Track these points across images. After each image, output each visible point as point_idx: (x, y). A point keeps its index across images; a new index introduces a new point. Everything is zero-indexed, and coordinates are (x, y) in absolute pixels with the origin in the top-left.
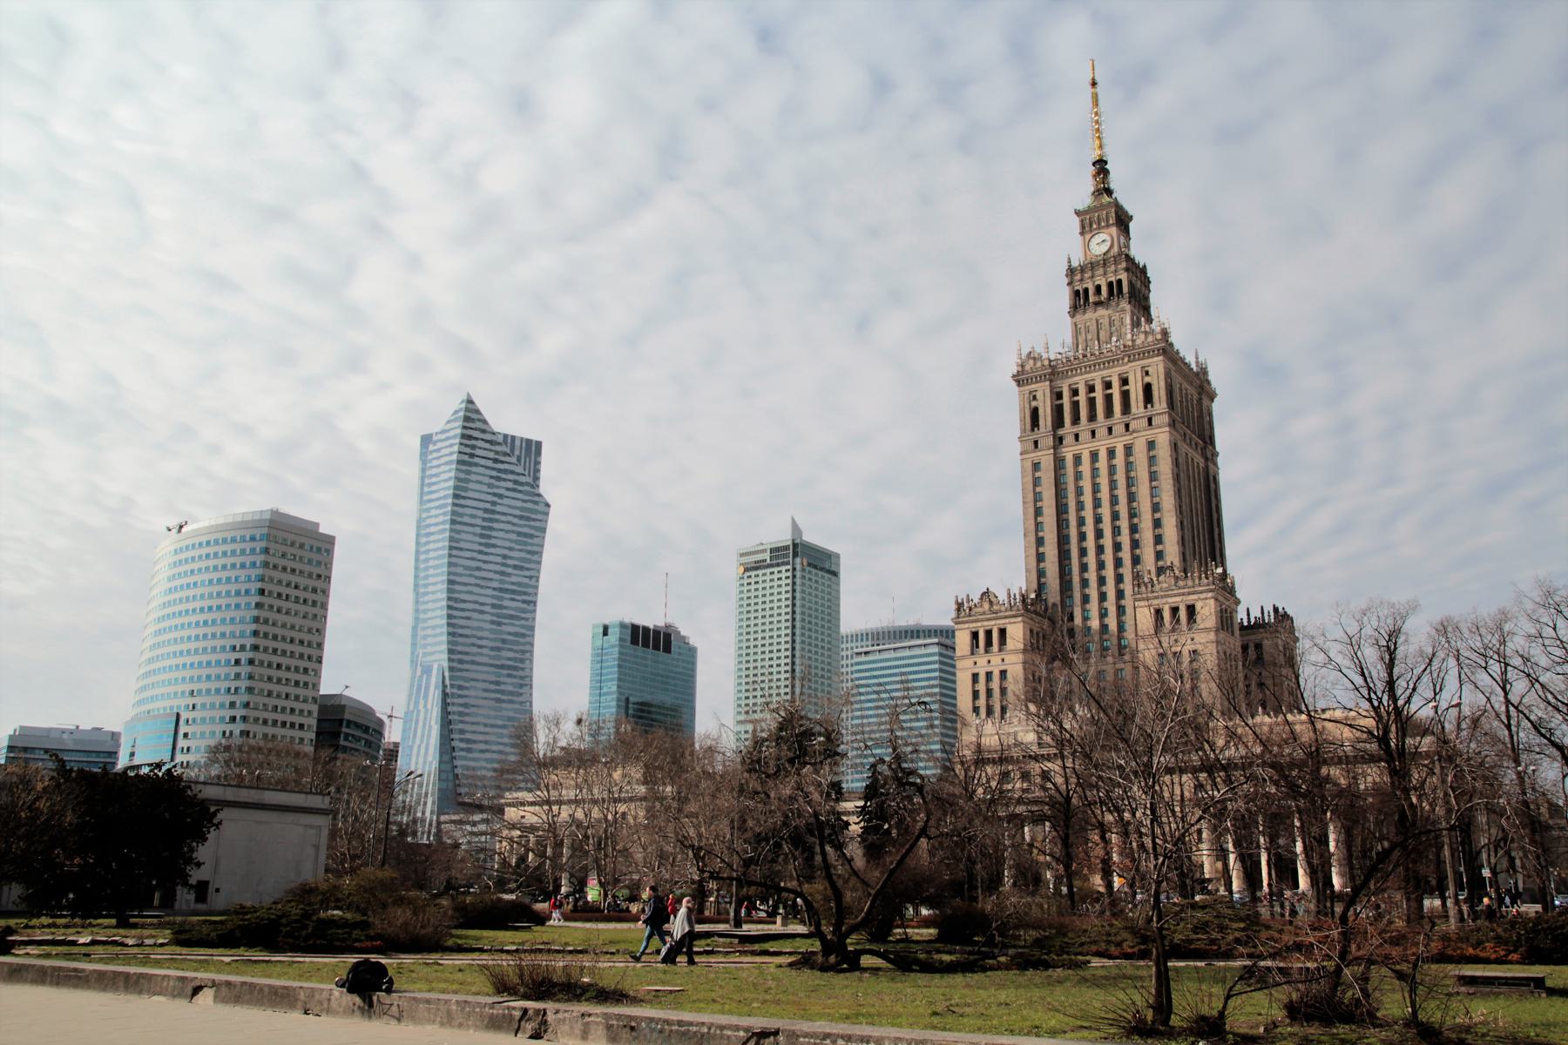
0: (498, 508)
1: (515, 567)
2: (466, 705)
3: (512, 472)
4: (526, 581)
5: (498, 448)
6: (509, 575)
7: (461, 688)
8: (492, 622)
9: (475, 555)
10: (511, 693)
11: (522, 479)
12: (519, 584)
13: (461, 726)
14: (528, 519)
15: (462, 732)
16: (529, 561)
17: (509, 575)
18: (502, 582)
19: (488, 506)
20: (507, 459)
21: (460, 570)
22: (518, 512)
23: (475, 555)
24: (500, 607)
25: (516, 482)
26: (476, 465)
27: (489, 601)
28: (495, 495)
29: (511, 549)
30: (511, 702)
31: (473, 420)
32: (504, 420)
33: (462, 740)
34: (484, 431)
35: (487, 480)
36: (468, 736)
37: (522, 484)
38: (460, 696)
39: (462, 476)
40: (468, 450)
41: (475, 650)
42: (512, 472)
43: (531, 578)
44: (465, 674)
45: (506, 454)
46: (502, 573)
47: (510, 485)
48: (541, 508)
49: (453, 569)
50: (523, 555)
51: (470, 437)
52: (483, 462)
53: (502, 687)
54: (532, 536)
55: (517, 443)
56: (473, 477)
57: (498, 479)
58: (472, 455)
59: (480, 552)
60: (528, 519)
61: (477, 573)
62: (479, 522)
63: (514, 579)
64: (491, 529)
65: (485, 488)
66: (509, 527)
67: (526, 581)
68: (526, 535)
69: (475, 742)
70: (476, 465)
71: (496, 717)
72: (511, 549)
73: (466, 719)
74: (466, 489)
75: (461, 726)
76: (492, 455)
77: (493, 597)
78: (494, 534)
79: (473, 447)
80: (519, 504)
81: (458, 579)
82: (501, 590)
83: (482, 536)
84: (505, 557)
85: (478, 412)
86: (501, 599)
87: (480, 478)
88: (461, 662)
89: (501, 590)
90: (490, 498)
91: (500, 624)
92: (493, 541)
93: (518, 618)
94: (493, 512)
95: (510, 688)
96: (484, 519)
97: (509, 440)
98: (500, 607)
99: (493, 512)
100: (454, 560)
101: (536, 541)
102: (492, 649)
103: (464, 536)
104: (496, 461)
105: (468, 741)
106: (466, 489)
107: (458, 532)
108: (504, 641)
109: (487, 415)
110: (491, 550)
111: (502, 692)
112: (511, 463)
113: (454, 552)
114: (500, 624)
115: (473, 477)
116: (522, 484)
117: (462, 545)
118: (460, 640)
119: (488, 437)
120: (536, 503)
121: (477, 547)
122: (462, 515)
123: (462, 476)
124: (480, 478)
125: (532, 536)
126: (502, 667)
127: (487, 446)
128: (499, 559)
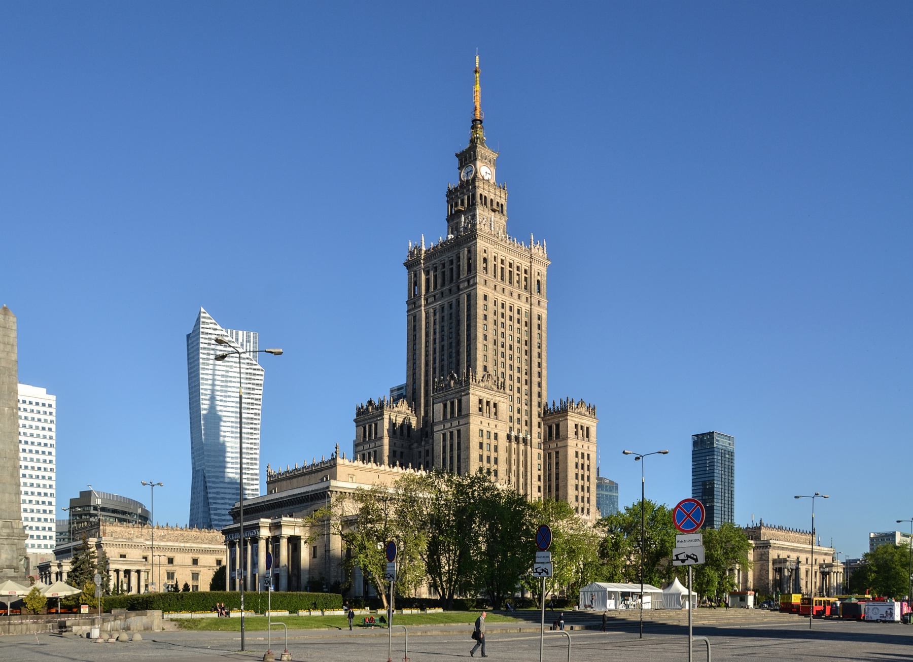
0: (230, 374)
2: (218, 493)
4: (252, 416)
13: (214, 506)
15: (216, 509)
19: (224, 373)
33: (215, 514)
36: (219, 511)
64: (226, 386)
67: (252, 416)
73: (218, 501)
75: (214, 506)
78: (229, 389)
90: (224, 368)
92: (229, 394)
94: (227, 376)
96: (222, 381)
99: (227, 376)
110: (228, 399)
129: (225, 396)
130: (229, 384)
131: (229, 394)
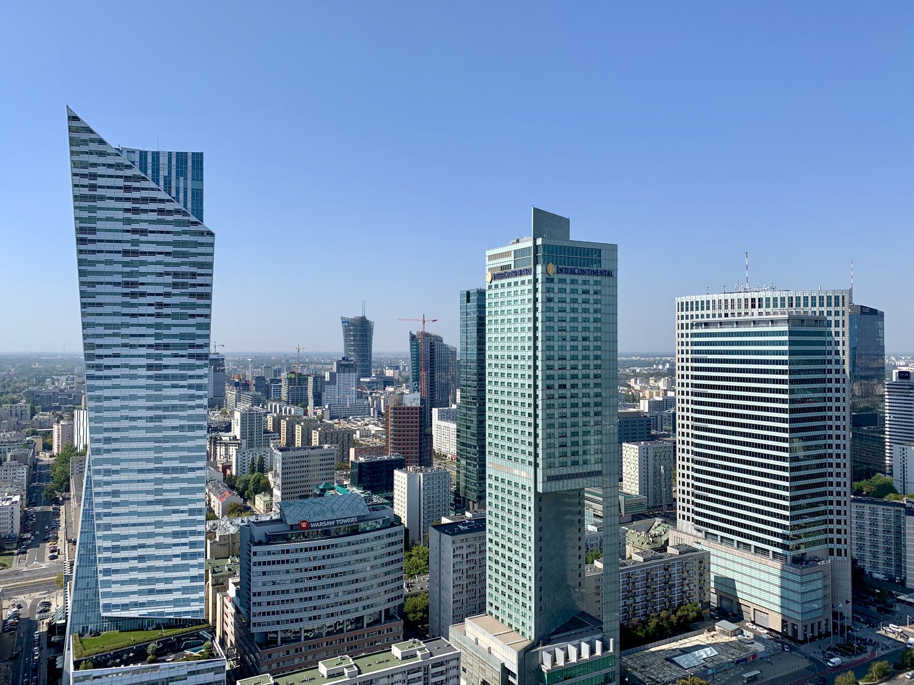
0: (143, 248)
2: (116, 493)
3: (154, 200)
4: (192, 330)
5: (128, 173)
6: (168, 327)
7: (108, 472)
8: (148, 387)
9: (118, 309)
10: (175, 470)
12: (182, 336)
13: (106, 520)
14: (184, 255)
15: (108, 527)
16: (194, 306)
17: (168, 327)
18: (157, 336)
19: (128, 247)
20: (144, 184)
21: (100, 330)
22: (170, 249)
23: (118, 309)
24: (159, 367)
25: (161, 211)
26: (102, 198)
28: (134, 231)
29: (167, 295)
30: (173, 480)
31: (85, 142)
32: (124, 131)
34: (102, 154)
35: (120, 215)
36: (115, 531)
37: (170, 212)
38: (108, 483)
39: (85, 214)
40: (86, 181)
41: (125, 424)
42: (154, 200)
43: (199, 326)
45: (137, 178)
46: (158, 326)
47: (154, 216)
48: (207, 239)
49: (90, 331)
50: (185, 299)
51: (86, 165)
53: (166, 464)
55: (163, 160)
56: (100, 214)
57: (135, 211)
58: (93, 187)
60: (184, 255)
61: (124, 331)
62: (119, 268)
63: (175, 331)
65: (120, 226)
66: (161, 269)
68: (184, 275)
69: (126, 537)
70: (102, 198)
71: (158, 502)
72: (167, 295)
73: (114, 510)
74: (93, 231)
75: (106, 520)
76: (120, 182)
77: (148, 356)
78: (142, 279)
79: (94, 176)
80: (170, 238)
82: (157, 346)
83: (127, 284)
84: (160, 305)
85: (89, 130)
86: (159, 357)
87: (110, 214)
88: (108, 440)
89: (157, 346)
92: (142, 289)
93: (183, 377)
94: (135, 253)
95: (176, 464)
96: (126, 264)
98: (159, 367)
99: (135, 253)
100: (91, 319)
101: (200, 280)
102: (150, 419)
103: (99, 288)
104: (127, 189)
106: (93, 231)
107: (93, 284)
108: (166, 408)
109: (101, 132)
110: (142, 300)
111: (166, 470)
112: (149, 188)
114: (159, 388)
115: (100, 214)
116: (170, 212)
118: (106, 414)
121: (119, 299)
122: (93, 263)
123: (85, 214)
124: (110, 214)
125: (194, 275)
126: (166, 440)
127: (112, 172)
128: (152, 310)
129: (133, 295)
130: (142, 269)
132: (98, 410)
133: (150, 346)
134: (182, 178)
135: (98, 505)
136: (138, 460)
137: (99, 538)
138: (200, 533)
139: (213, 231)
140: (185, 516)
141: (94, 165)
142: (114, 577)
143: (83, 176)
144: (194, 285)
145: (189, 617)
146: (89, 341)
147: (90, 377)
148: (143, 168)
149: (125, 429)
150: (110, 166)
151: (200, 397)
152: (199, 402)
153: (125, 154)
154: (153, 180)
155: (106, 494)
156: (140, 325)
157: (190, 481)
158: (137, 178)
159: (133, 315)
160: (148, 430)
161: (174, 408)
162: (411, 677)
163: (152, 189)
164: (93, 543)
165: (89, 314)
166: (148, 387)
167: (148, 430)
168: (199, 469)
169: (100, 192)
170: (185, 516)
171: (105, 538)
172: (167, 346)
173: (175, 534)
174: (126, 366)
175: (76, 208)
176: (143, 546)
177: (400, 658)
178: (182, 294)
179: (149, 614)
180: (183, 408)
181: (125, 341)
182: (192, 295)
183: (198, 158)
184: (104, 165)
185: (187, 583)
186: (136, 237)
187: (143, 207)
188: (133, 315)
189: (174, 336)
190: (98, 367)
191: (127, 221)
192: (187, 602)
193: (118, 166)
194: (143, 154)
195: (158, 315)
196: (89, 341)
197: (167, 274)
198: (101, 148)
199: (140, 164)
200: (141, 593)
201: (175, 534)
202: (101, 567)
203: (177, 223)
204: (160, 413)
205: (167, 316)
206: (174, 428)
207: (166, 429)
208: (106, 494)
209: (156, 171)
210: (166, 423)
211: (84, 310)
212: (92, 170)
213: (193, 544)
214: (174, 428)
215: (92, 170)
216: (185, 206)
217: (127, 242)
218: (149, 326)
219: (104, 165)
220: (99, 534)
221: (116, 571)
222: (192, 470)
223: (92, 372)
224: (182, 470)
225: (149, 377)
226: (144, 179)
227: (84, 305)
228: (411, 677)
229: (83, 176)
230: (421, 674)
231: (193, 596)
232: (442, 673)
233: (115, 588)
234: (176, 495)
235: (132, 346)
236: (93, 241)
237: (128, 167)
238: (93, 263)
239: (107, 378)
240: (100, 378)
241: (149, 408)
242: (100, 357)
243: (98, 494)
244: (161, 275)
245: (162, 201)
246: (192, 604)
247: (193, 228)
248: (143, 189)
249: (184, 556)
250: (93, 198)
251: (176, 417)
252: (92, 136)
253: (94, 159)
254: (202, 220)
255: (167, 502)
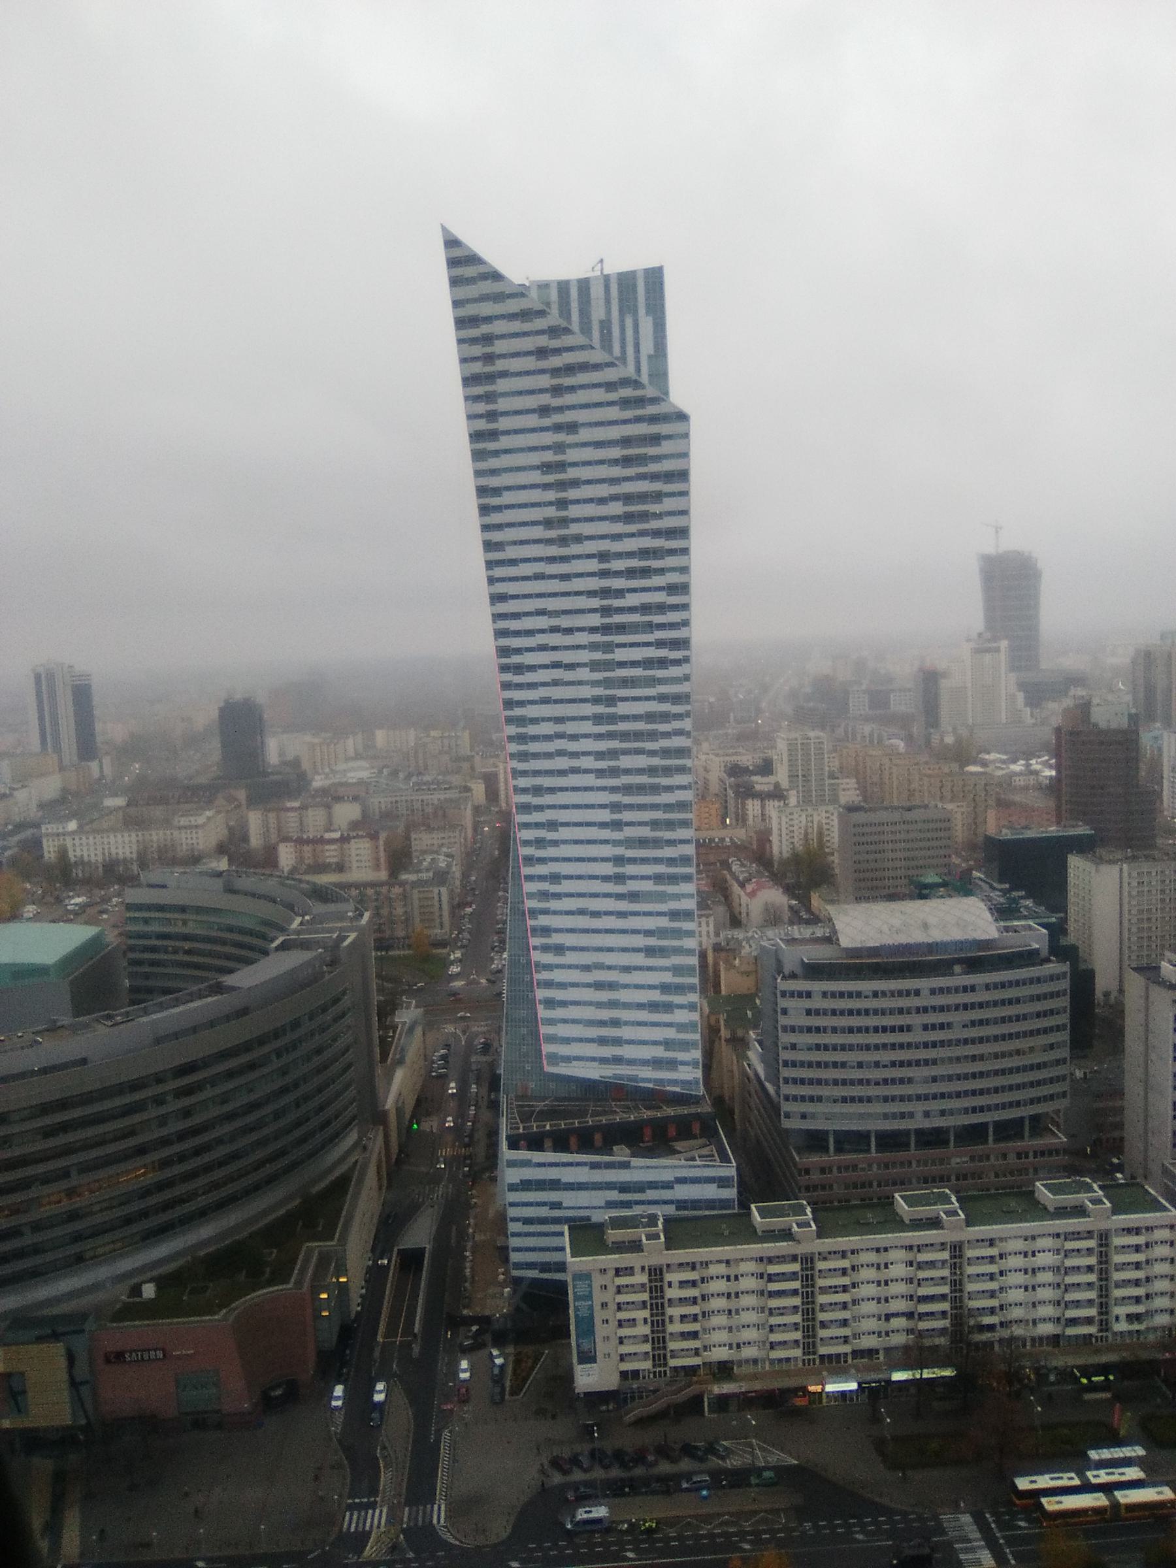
0: (572, 455)
1: (631, 573)
2: (555, 878)
3: (584, 367)
6: (620, 593)
7: (540, 843)
8: (596, 700)
11: (611, 375)
12: (645, 609)
13: (543, 921)
15: (546, 931)
17: (620, 593)
18: (606, 611)
19: (549, 456)
20: (568, 341)
22: (616, 453)
26: (504, 374)
27: (584, 656)
28: (558, 428)
34: (499, 297)
36: (556, 939)
40: (477, 350)
41: (562, 763)
42: (584, 367)
43: (672, 589)
44: (549, 815)
46: (605, 593)
49: (503, 608)
52: (515, 365)
54: (658, 497)
55: (597, 292)
57: (557, 390)
58: (489, 358)
59: (552, 560)
63: (632, 600)
65: (533, 421)
66: (603, 491)
68: (643, 497)
75: (543, 921)
77: (594, 647)
79: (488, 339)
80: (615, 433)
81: (514, 625)
82: (606, 629)
84: (603, 556)
85: (473, 259)
86: (608, 647)
88: (538, 790)
89: (606, 629)
90: (549, 438)
91: (611, 701)
92: (574, 529)
93: (653, 682)
95: (645, 832)
97: (572, 295)
100: (501, 588)
101: (669, 504)
102: (600, 755)
105: (560, 949)
106: (494, 435)
108: (625, 736)
109: (495, 258)
110: (575, 549)
113: (499, 572)
114: (611, 701)
115: (502, 405)
117: (511, 553)
118: (534, 747)
119: (513, 306)
120: (653, 419)
122: (497, 491)
123: (481, 408)
125: (658, 497)
126: (627, 789)
127: (516, 326)
128: (593, 565)
129: (563, 541)
131: (574, 529)
132: (522, 738)
133: (593, 630)
134: (629, 322)
135: (531, 896)
136: (589, 824)
137: (535, 948)
138: (690, 952)
139: (686, 409)
140: (664, 922)
141: (488, 319)
142: (559, 1013)
143: (473, 341)
144: (659, 516)
145: (678, 1089)
146: (503, 624)
147: (506, 686)
148: (565, 312)
149: (562, 773)
150: (512, 317)
151: (679, 717)
152: (676, 725)
153: (534, 294)
154: (582, 333)
155: (542, 878)
156: (578, 593)
157: (671, 862)
158: (553, 332)
159: (565, 577)
160: (600, 773)
161: (638, 736)
162: (1070, 1245)
163: (582, 348)
164: (528, 954)
165: (503, 580)
166: (596, 700)
167: (600, 773)
168: (682, 842)
169: (500, 365)
170: (664, 922)
171: (545, 948)
172: (621, 628)
173: (650, 951)
174: (556, 665)
175: (467, 398)
176: (600, 966)
177: (1051, 1209)
178: (642, 533)
179: (615, 1076)
180: (653, 736)
181: (554, 622)
182: (657, 533)
183: (655, 278)
184: (502, 317)
185: (671, 1033)
186: (561, 437)
187: (568, 381)
188: (565, 577)
189: (631, 610)
190: (519, 669)
191: (544, 411)
192: (672, 1064)
193: (525, 315)
194: (563, 287)
195: (604, 574)
196: (503, 624)
197: (615, 498)
198: (496, 287)
199: (560, 305)
200: (602, 1041)
201: (650, 951)
202: (541, 994)
203: (625, 403)
204: (615, 744)
205: (618, 574)
206: (640, 771)
207: (627, 772)
208: (542, 878)
209: (585, 313)
210: (625, 762)
211: (491, 573)
212: (485, 329)
213: (677, 970)
214: (640, 771)
215: (485, 329)
216: (638, 370)
217: (548, 448)
218: (591, 594)
219: (502, 317)
220: (534, 941)
221: (564, 1004)
222: (671, 843)
223: (508, 677)
224: (657, 843)
225: (595, 683)
226: (567, 331)
227: (490, 564)
228: (1070, 1245)
229: (473, 341)
230: (1092, 1243)
231: (681, 1056)
232: (1137, 1249)
233: (562, 1031)
234: (648, 886)
235: (569, 631)
236: (496, 453)
237: (541, 313)
238: (497, 491)
239: (532, 686)
240: (520, 686)
241: (599, 737)
242: (518, 651)
243: (530, 878)
244: (602, 501)
245: (597, 367)
246: (681, 1068)
247: (651, 410)
248: (570, 349)
249: (665, 988)
250: (491, 378)
251: (639, 752)
252: (482, 269)
253: (487, 309)
254: (667, 393)
255: (634, 896)
